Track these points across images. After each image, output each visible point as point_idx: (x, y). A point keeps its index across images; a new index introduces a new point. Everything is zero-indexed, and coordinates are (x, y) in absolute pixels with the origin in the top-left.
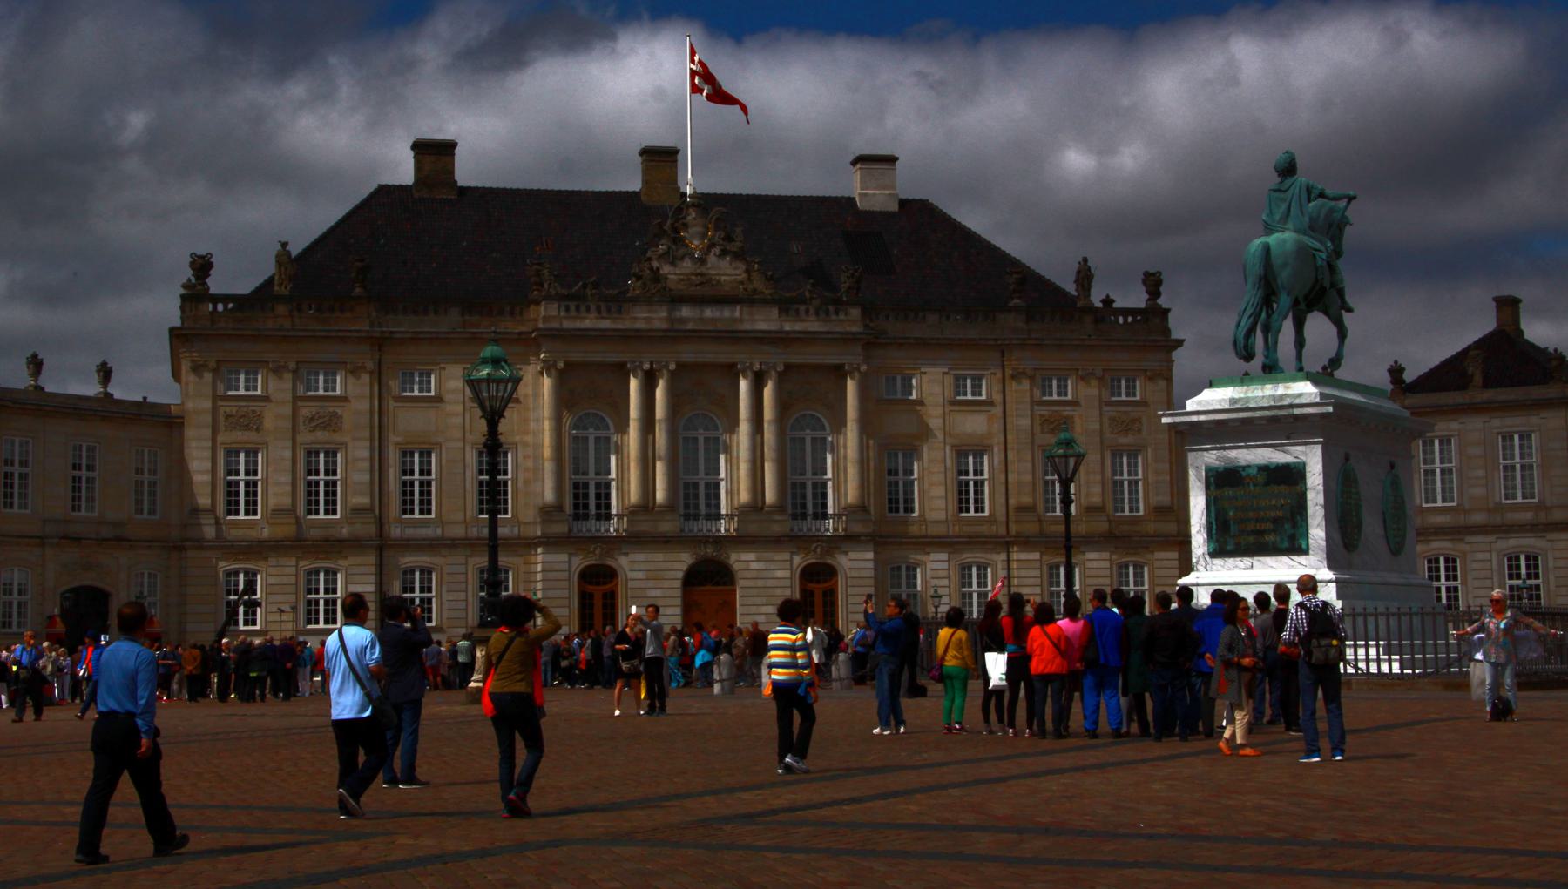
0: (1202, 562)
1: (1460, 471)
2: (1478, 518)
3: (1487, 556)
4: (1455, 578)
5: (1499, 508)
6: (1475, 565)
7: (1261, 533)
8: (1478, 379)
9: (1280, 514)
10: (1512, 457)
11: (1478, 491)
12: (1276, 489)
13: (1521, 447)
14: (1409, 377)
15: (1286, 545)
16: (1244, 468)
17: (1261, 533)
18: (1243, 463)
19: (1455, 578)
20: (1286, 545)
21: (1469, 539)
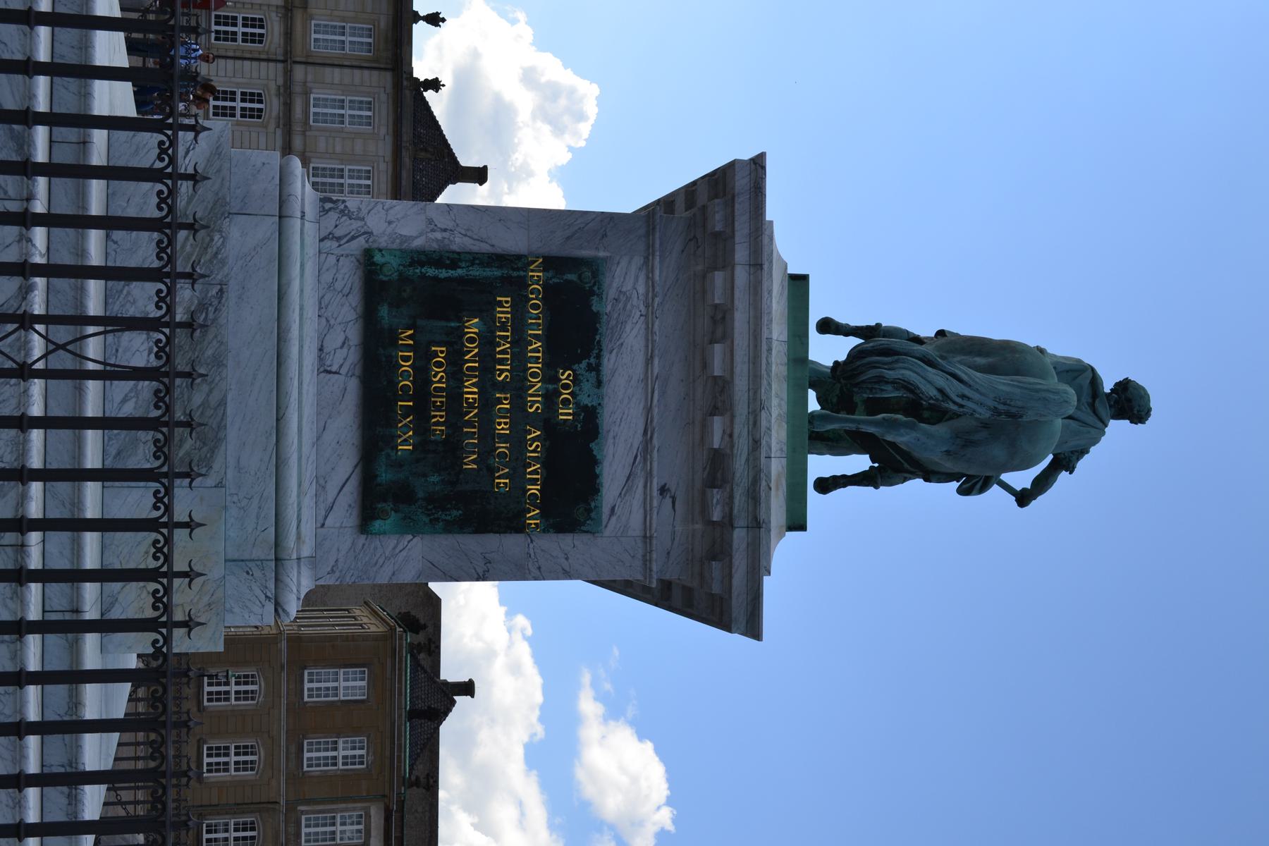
0: (348, 226)
1: (341, 130)
4: (242, 116)
6: (254, 135)
7: (421, 412)
9: (470, 463)
10: (351, 177)
11: (322, 145)
12: (534, 449)
13: (360, 186)
14: (429, 95)
15: (385, 476)
16: (596, 369)
17: (421, 412)
18: (608, 363)
19: (242, 116)
20: (385, 476)
21: (279, 132)
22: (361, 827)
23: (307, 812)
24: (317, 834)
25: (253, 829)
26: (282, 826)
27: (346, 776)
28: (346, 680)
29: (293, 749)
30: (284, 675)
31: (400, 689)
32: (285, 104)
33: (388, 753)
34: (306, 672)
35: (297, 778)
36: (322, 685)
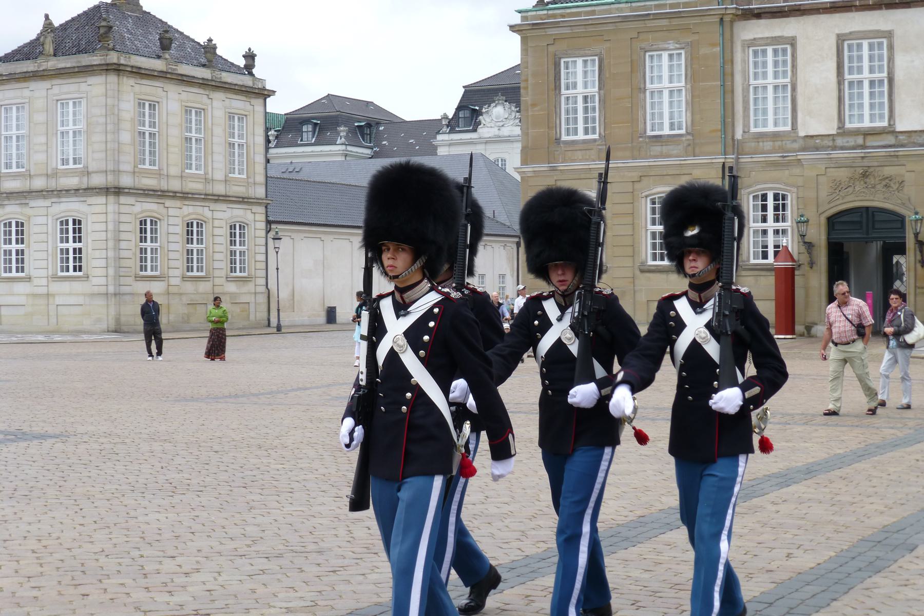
2: (39, 183)
3: (42, 220)
5: (55, 174)
8: (49, 48)
11: (40, 157)
21: (32, 203)
22: (770, 50)
23: (746, 125)
24: (575, 111)
25: (764, 197)
26: (759, 158)
27: (693, 76)
28: (575, 86)
29: (657, 149)
30: (561, 166)
31: (587, 13)
32: (8, 198)
33: (665, 22)
34: (564, 138)
35: (692, 142)
36: (580, 115)
